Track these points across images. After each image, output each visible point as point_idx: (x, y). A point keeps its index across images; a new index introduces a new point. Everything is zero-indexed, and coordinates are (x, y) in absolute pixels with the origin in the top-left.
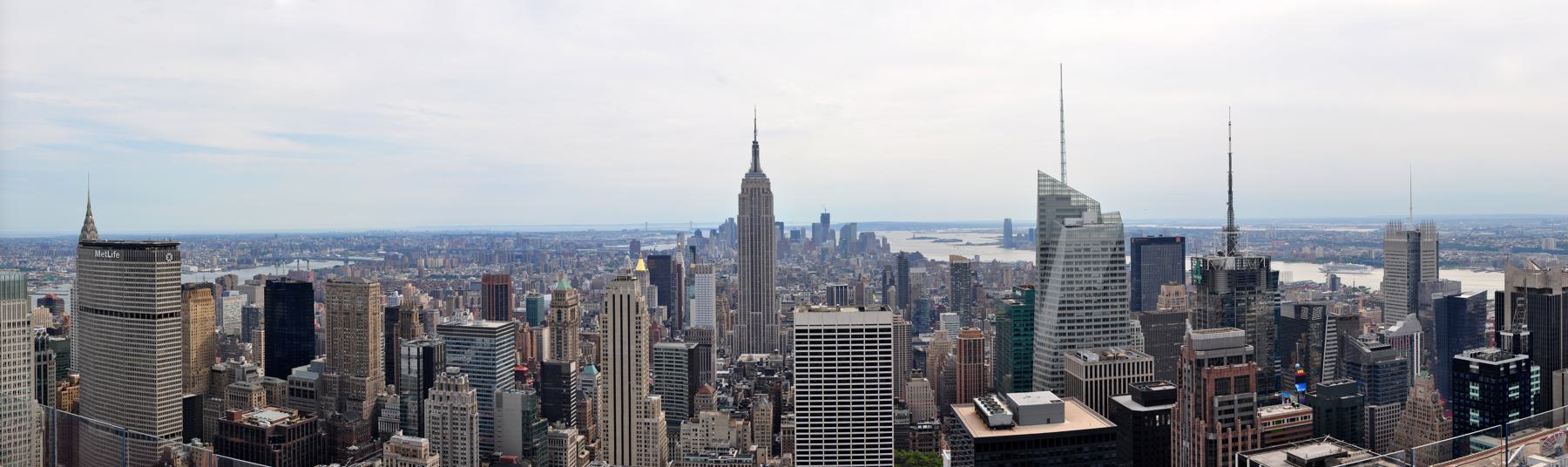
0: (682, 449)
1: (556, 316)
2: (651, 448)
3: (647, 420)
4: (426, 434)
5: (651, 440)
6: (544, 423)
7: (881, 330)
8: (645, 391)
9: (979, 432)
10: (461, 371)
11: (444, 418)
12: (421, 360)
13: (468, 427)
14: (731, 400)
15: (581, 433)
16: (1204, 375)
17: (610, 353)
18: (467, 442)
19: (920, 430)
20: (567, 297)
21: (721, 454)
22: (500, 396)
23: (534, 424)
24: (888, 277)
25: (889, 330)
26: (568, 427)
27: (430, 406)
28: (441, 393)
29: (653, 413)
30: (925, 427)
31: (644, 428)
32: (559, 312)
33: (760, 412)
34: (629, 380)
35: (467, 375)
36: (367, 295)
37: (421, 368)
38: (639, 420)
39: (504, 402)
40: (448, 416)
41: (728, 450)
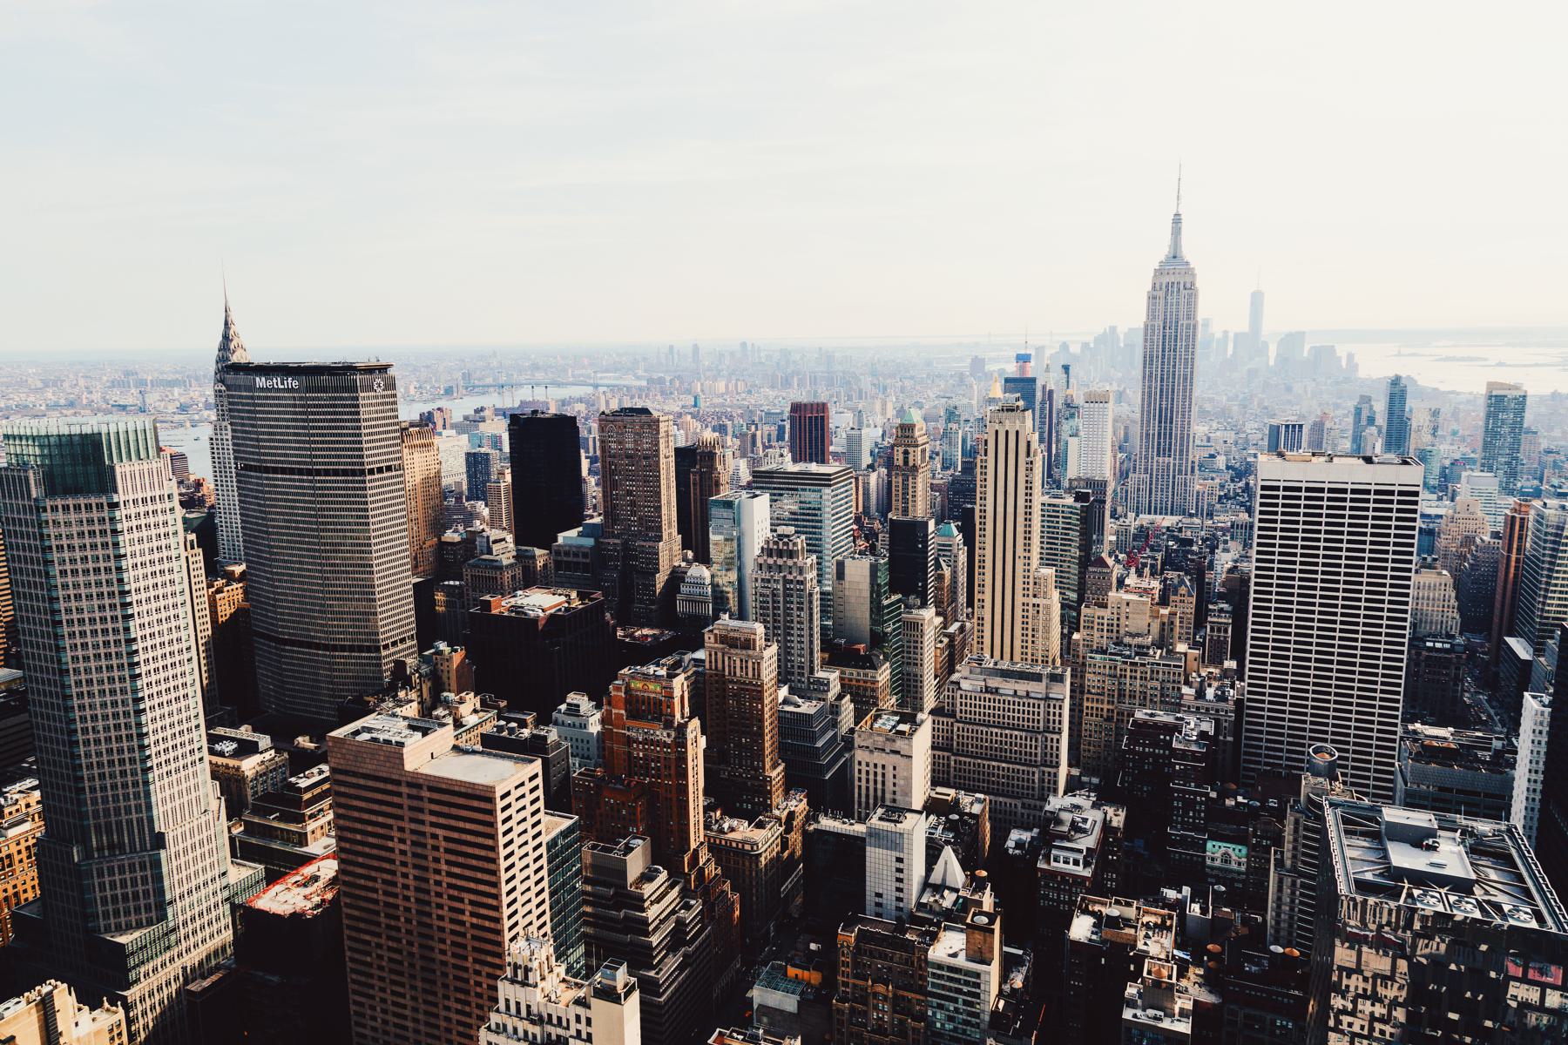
0: (1081, 643)
1: (901, 457)
3: (1036, 601)
6: (899, 601)
8: (1035, 561)
10: (796, 532)
11: (774, 595)
13: (805, 606)
15: (938, 614)
17: (990, 509)
18: (806, 626)
19: (1433, 649)
20: (917, 433)
21: (1137, 654)
22: (840, 566)
23: (886, 602)
25: (1416, 494)
26: (924, 605)
28: (770, 561)
29: (1045, 593)
30: (1438, 645)
32: (906, 453)
33: (1178, 598)
35: (803, 537)
36: (658, 433)
38: (1026, 600)
39: (847, 571)
40: (781, 592)
41: (1148, 648)
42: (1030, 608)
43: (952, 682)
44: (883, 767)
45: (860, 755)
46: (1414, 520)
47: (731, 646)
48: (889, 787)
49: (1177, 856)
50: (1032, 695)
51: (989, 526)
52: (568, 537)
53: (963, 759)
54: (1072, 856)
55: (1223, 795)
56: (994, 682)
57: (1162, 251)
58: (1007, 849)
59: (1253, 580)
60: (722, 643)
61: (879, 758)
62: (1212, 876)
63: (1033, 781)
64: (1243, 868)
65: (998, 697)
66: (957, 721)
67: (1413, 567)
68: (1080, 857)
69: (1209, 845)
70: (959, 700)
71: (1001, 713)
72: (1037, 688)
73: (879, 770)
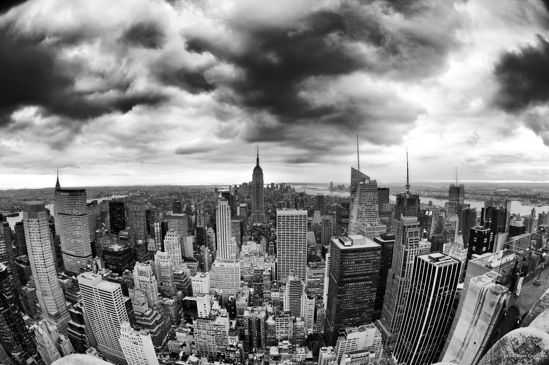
1: (199, 212)
3: (231, 244)
4: (165, 250)
7: (304, 216)
8: (230, 236)
9: (342, 247)
14: (253, 238)
15: (209, 249)
16: (406, 231)
19: (311, 247)
24: (297, 200)
25: (306, 216)
31: (231, 247)
32: (200, 211)
35: (176, 231)
38: (229, 244)
45: (193, 282)
46: (306, 221)
48: (201, 290)
52: (122, 232)
53: (217, 282)
54: (243, 300)
55: (274, 282)
56: (223, 264)
57: (255, 165)
58: (229, 300)
59: (277, 236)
64: (279, 297)
67: (307, 231)
69: (272, 293)
70: (215, 269)
72: (233, 265)
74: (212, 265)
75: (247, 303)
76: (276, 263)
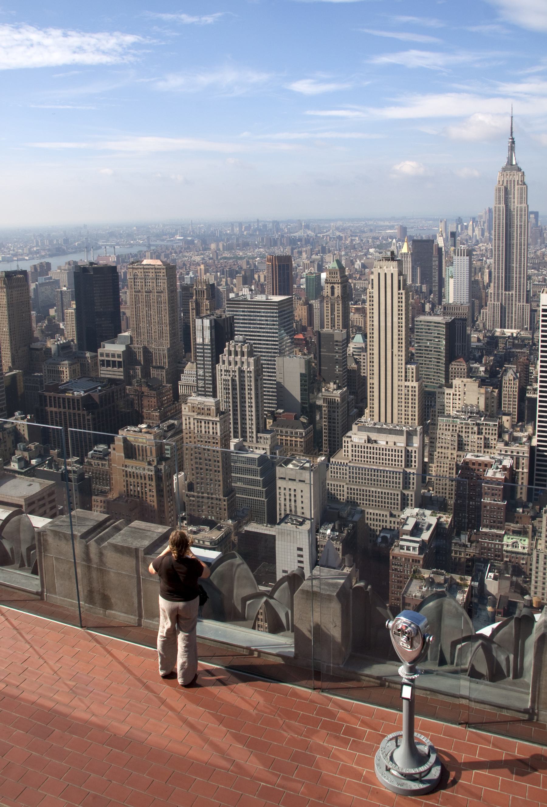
1: (329, 291)
2: (410, 409)
3: (407, 383)
5: (410, 401)
12: (213, 330)
27: (221, 370)
32: (333, 288)
34: (392, 348)
37: (214, 337)
38: (400, 383)
42: (403, 388)
43: (348, 437)
44: (295, 490)
45: (280, 483)
47: (199, 414)
49: (486, 545)
50: (398, 444)
51: (376, 335)
60: (194, 411)
61: (292, 485)
62: (507, 557)
63: (398, 500)
64: (526, 551)
65: (375, 445)
66: (350, 462)
68: (417, 545)
71: (378, 456)
73: (292, 493)
74: (344, 439)
75: (422, 556)
76: (532, 449)
